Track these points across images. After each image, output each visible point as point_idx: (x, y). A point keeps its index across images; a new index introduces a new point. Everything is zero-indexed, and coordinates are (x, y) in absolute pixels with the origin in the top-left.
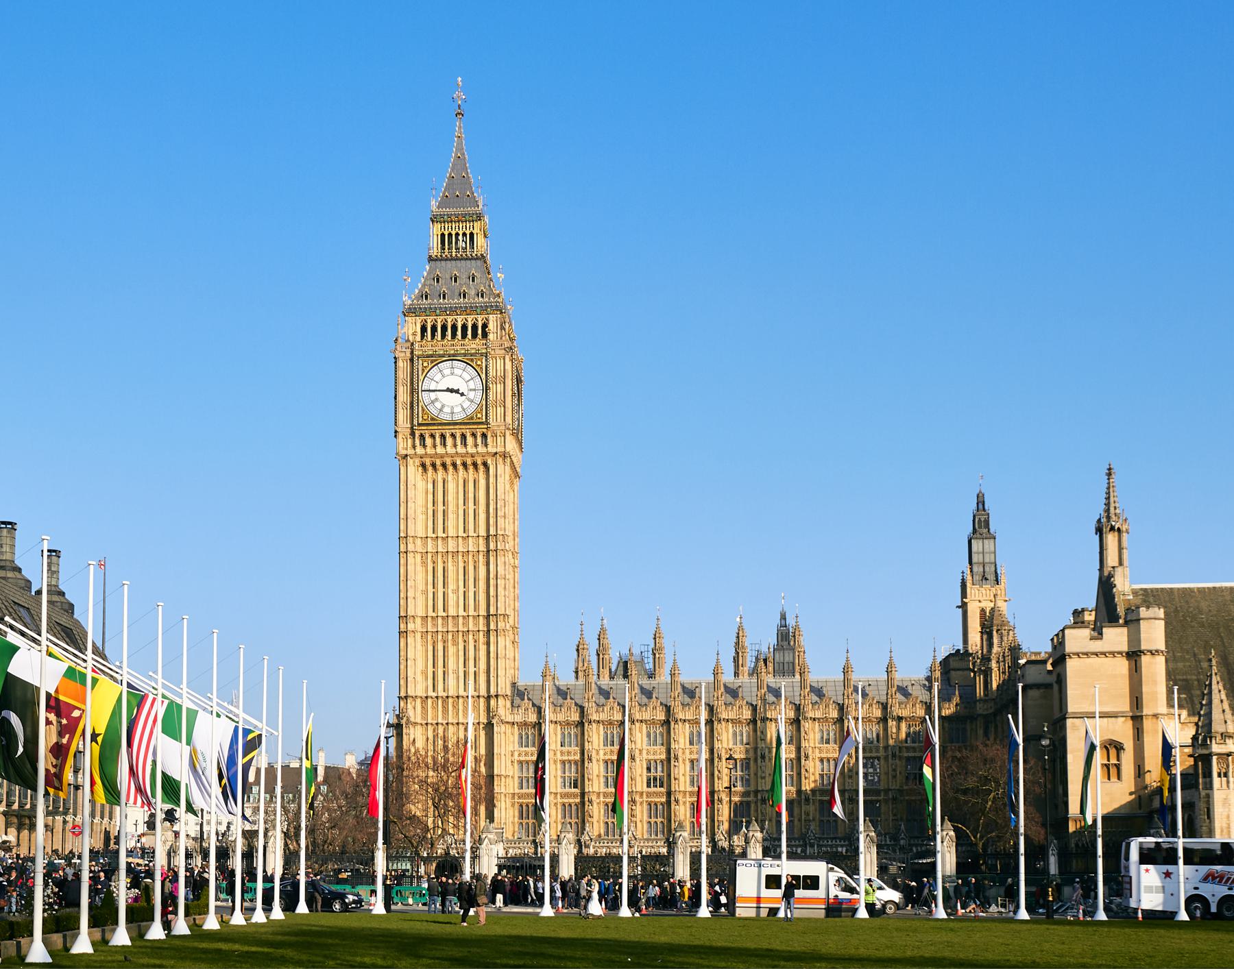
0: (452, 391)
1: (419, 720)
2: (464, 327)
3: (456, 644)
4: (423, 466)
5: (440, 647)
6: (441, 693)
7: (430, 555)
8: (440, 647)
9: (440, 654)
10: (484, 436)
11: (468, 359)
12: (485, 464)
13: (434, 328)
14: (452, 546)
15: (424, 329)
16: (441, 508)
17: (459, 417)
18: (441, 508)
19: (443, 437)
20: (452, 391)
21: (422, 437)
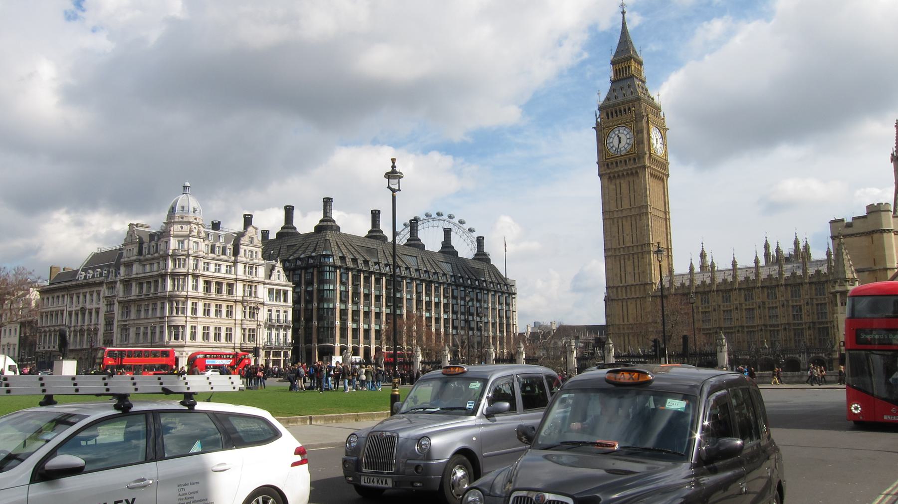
0: (620, 142)
1: (615, 297)
2: (625, 110)
3: (629, 259)
4: (610, 177)
5: (622, 262)
6: (624, 284)
7: (616, 221)
8: (622, 262)
9: (623, 265)
10: (634, 159)
11: (626, 124)
12: (637, 172)
13: (612, 114)
14: (625, 214)
15: (607, 115)
16: (619, 196)
17: (623, 153)
18: (619, 196)
19: (616, 163)
20: (620, 142)
21: (608, 165)
